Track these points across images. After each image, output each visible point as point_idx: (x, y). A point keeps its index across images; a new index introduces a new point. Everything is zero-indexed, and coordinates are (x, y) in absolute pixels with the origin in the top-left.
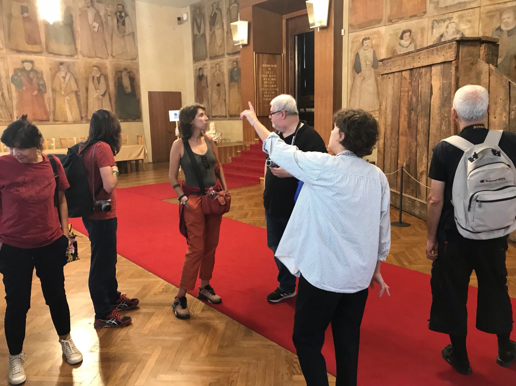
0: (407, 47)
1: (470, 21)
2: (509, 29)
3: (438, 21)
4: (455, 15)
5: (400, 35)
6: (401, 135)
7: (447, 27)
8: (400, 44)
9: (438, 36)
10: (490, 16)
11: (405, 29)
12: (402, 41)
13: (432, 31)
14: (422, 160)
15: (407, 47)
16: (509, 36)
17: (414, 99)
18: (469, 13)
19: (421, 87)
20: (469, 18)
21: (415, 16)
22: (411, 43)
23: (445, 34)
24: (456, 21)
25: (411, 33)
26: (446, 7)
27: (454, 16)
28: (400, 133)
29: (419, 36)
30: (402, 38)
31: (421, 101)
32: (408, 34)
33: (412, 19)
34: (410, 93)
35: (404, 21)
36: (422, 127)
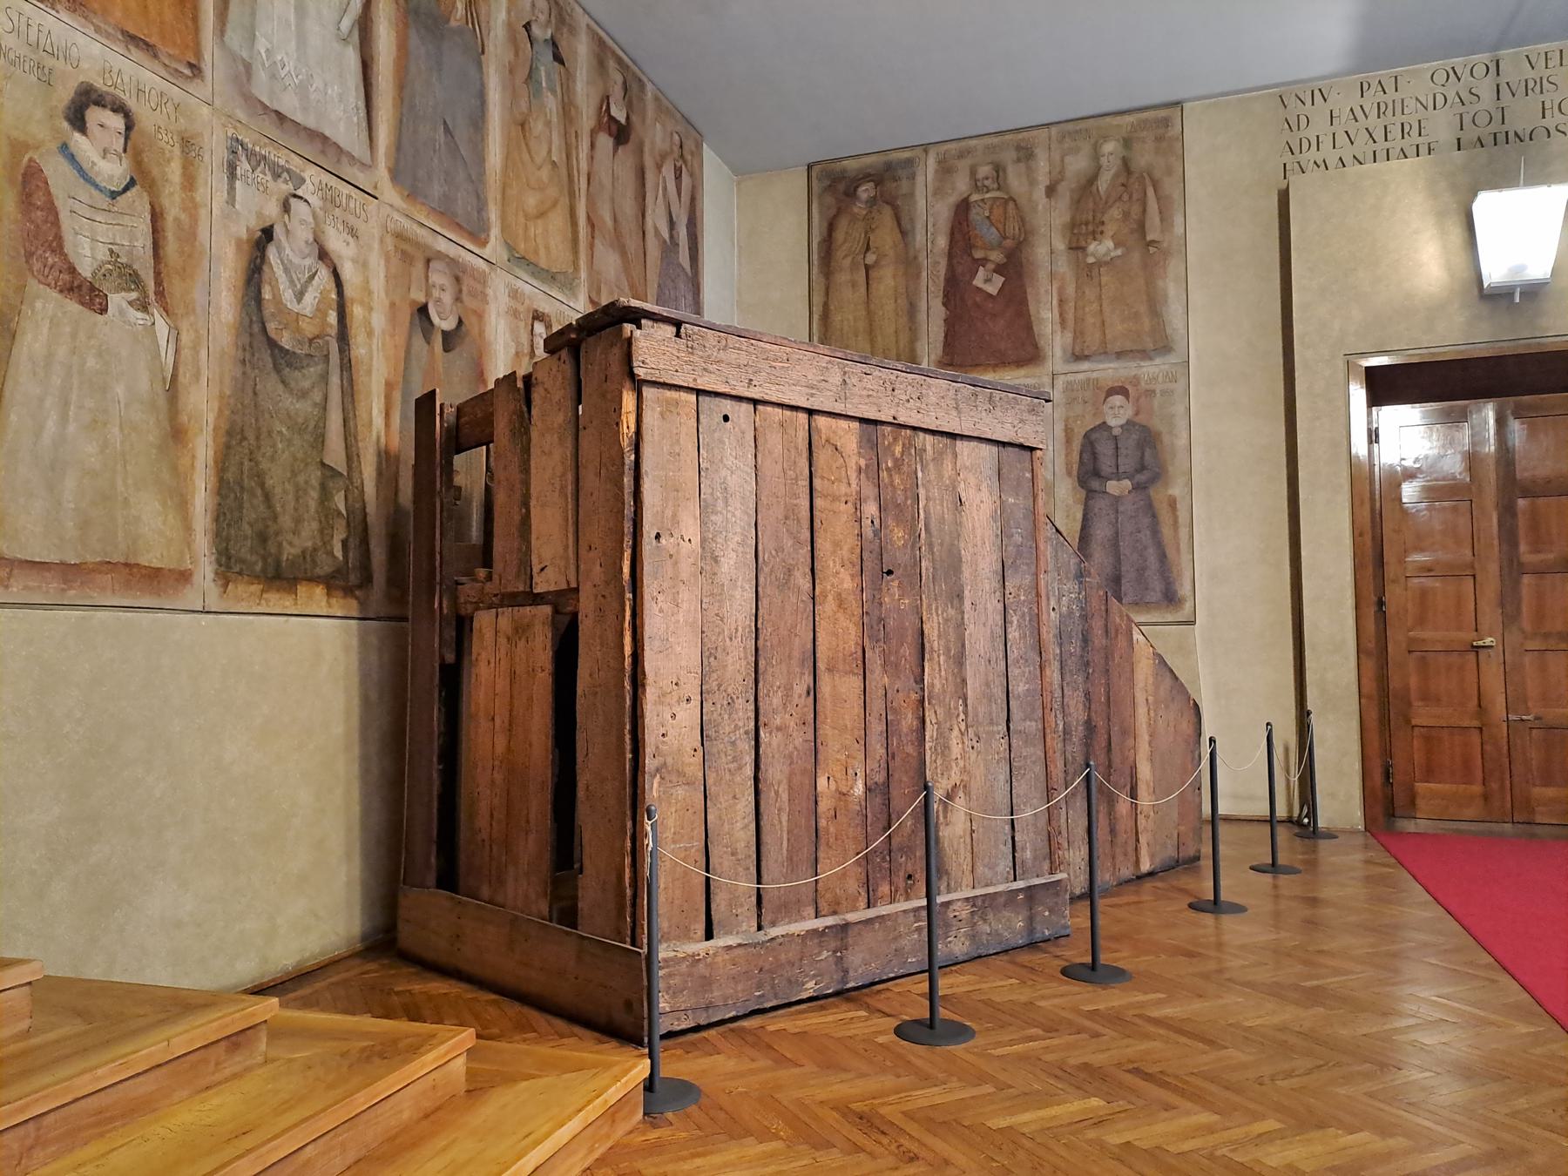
0: (114, 195)
1: (353, 232)
2: (448, 324)
3: (257, 160)
4: (311, 173)
5: (64, 94)
6: (829, 670)
7: (286, 208)
8: (64, 148)
9: (256, 225)
10: (404, 253)
11: (98, 84)
12: (77, 135)
13: (232, 189)
14: (947, 747)
15: (114, 195)
16: (447, 349)
17: (898, 535)
18: (349, 197)
19: (927, 499)
20: (352, 220)
21: (148, 48)
22: (132, 183)
23: (278, 231)
24: (315, 201)
25: (129, 127)
26: (281, 117)
27: (306, 175)
28: (821, 665)
29: (174, 171)
30: (77, 119)
31: (931, 545)
32: (118, 122)
33: (136, 54)
34: (871, 509)
35: (90, 31)
36: (939, 636)
